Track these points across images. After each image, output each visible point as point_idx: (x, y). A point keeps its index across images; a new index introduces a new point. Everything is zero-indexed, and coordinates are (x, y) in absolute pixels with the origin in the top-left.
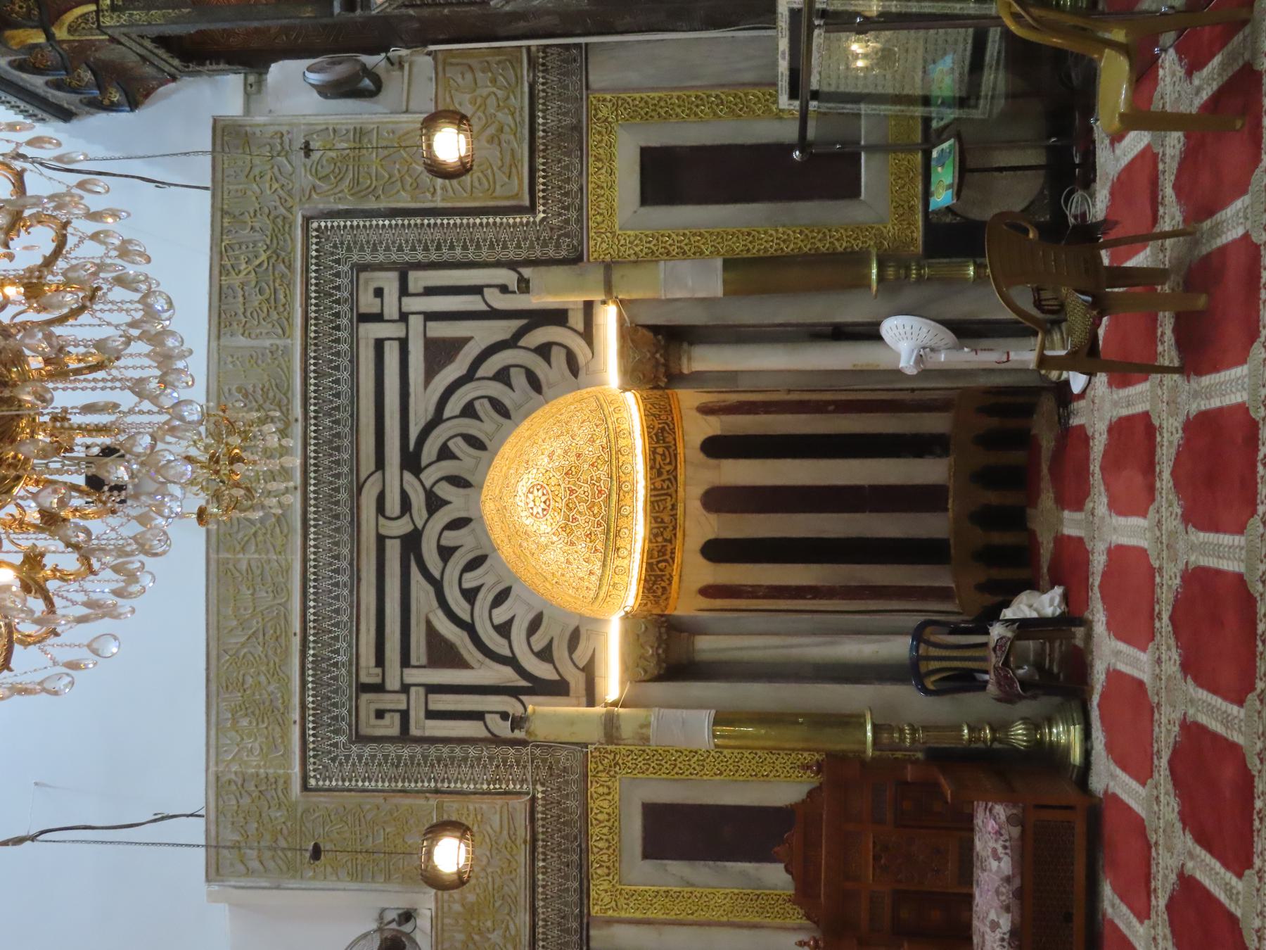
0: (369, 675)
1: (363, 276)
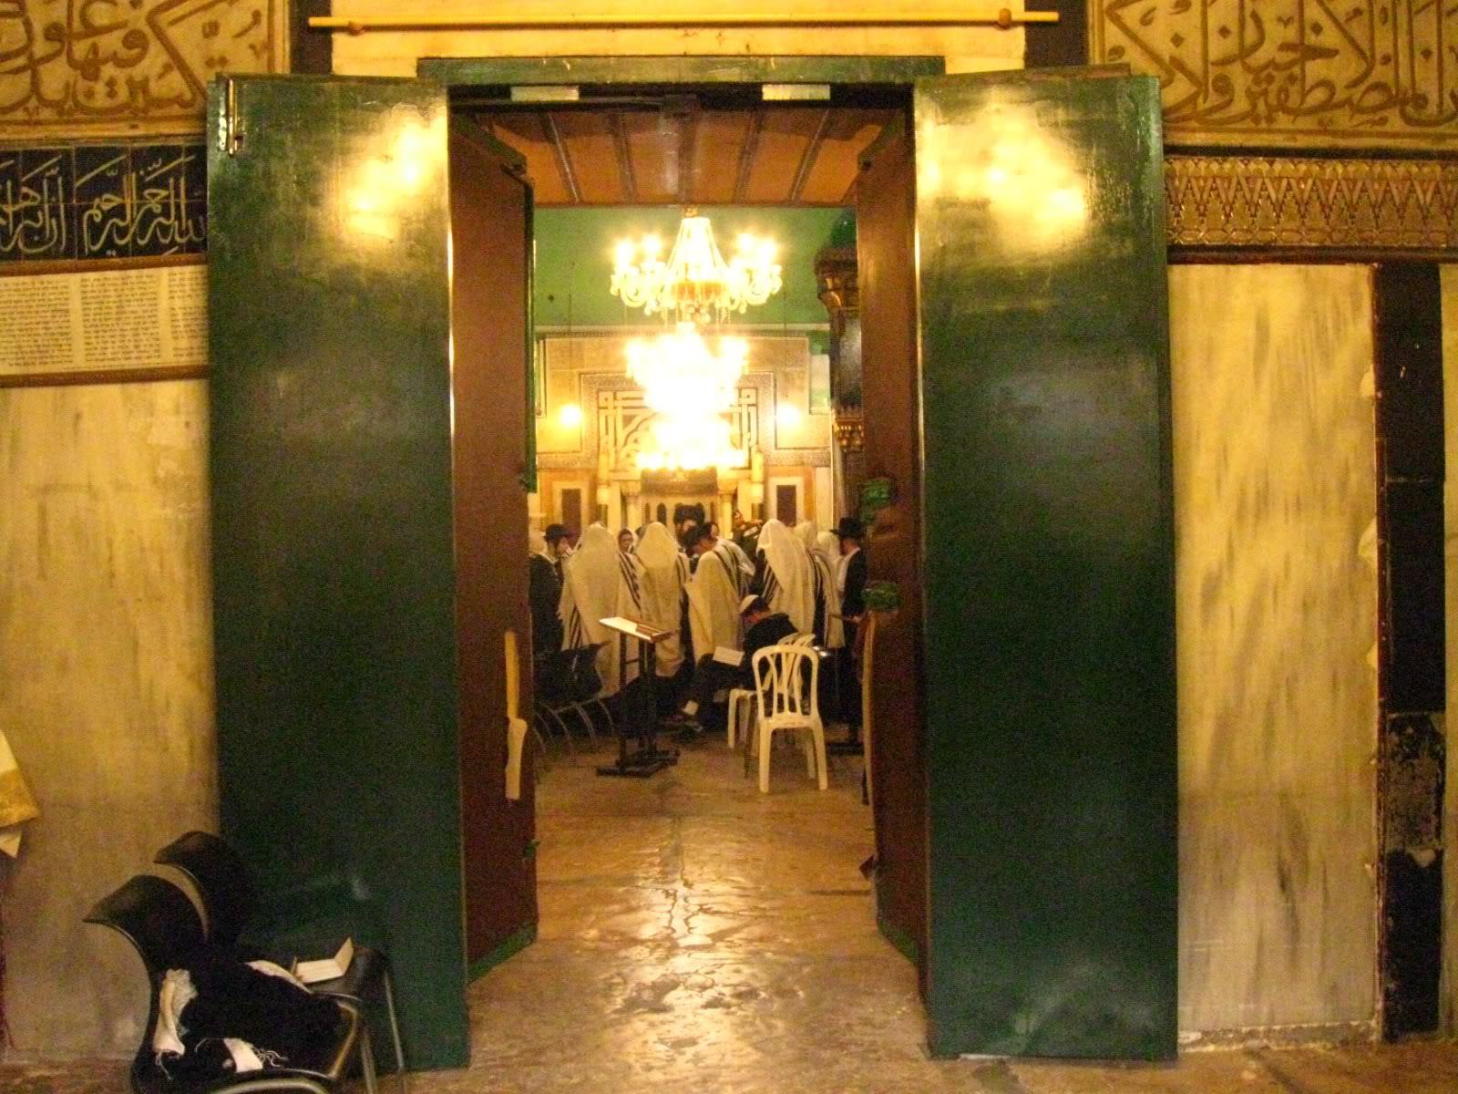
0: (619, 395)
1: (754, 391)
